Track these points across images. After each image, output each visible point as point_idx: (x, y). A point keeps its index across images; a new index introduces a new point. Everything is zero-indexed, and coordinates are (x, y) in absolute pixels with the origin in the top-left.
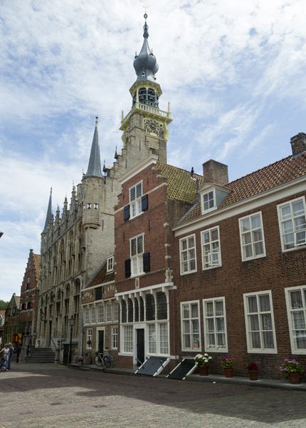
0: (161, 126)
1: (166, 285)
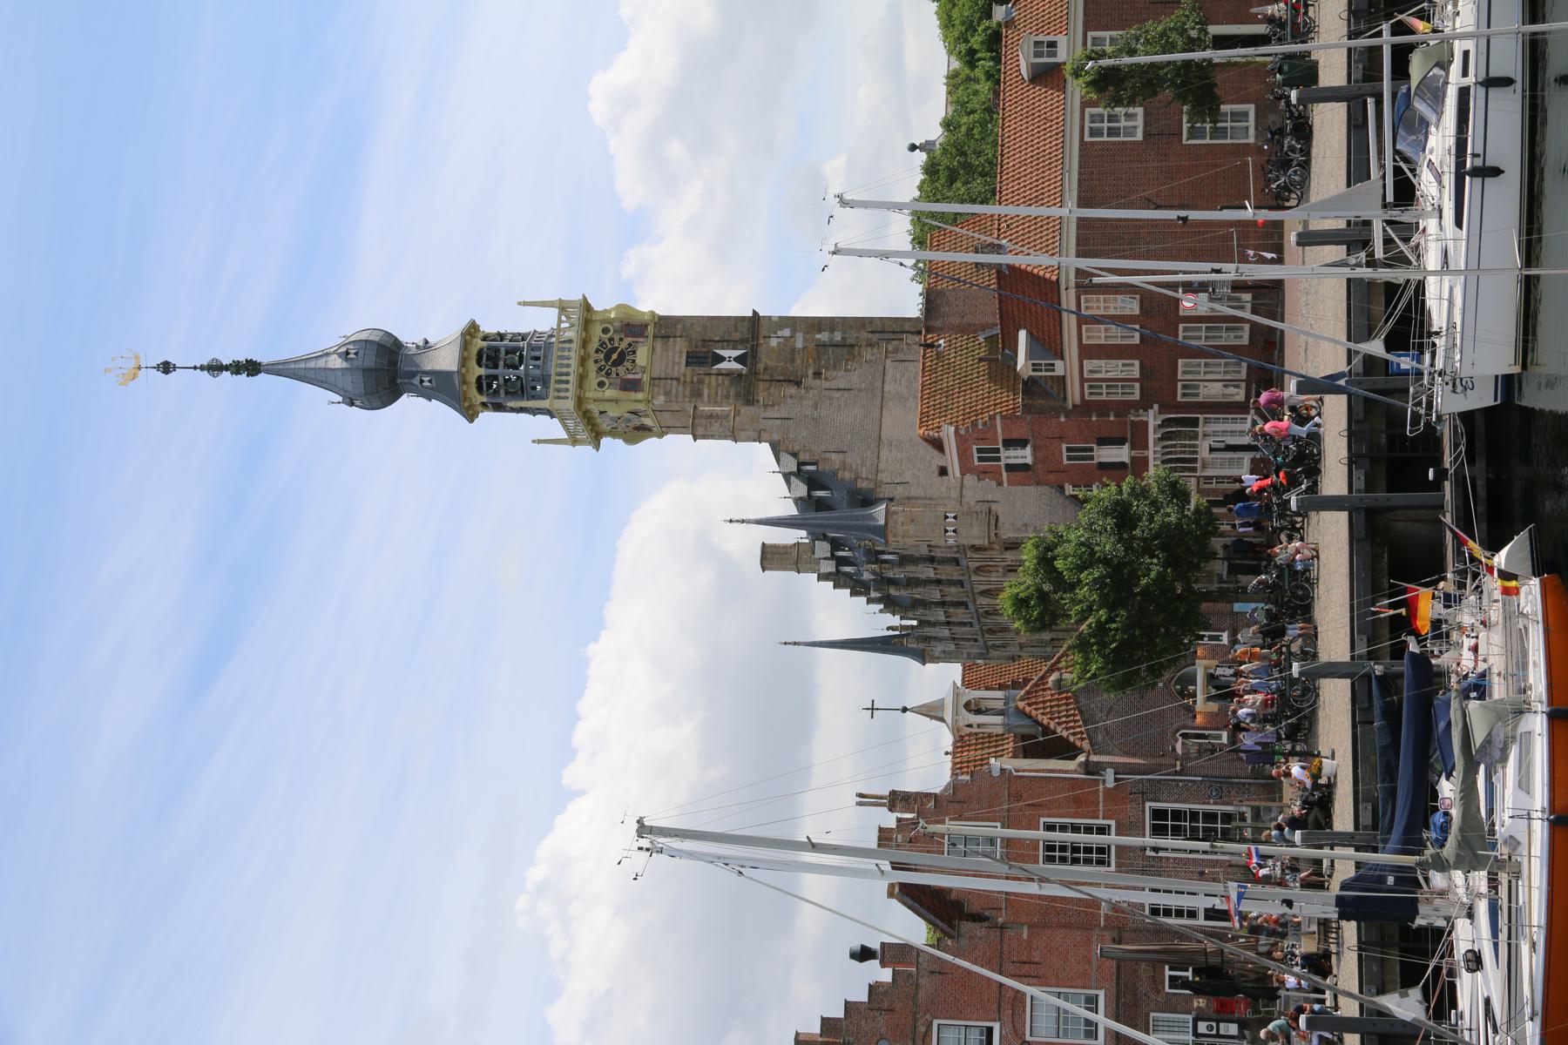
0: (605, 331)
1: (1153, 418)
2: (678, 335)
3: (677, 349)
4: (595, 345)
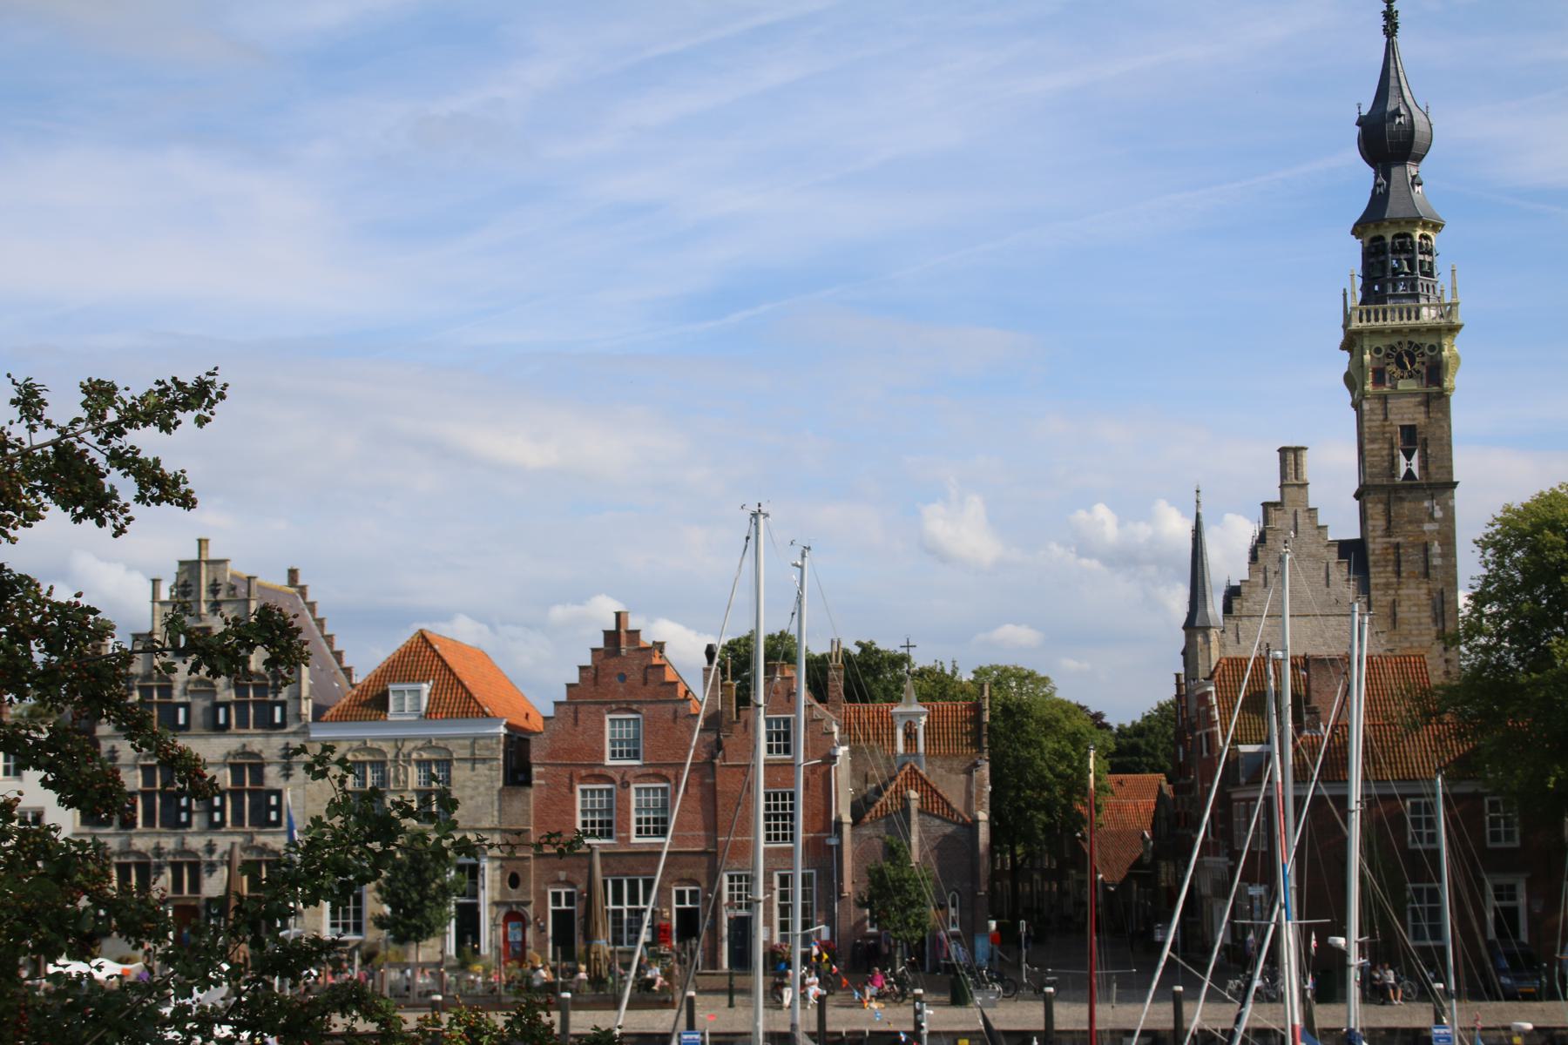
0: (1432, 348)
2: (1431, 415)
3: (1417, 416)
4: (1416, 340)
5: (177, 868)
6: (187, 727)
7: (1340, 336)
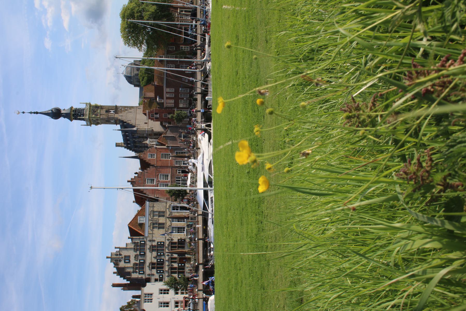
4: (91, 109)
5: (172, 262)
6: (144, 260)
7: (89, 127)
